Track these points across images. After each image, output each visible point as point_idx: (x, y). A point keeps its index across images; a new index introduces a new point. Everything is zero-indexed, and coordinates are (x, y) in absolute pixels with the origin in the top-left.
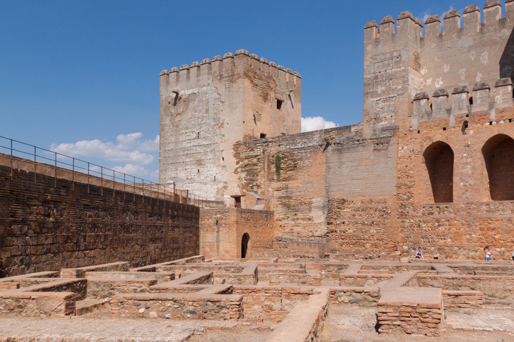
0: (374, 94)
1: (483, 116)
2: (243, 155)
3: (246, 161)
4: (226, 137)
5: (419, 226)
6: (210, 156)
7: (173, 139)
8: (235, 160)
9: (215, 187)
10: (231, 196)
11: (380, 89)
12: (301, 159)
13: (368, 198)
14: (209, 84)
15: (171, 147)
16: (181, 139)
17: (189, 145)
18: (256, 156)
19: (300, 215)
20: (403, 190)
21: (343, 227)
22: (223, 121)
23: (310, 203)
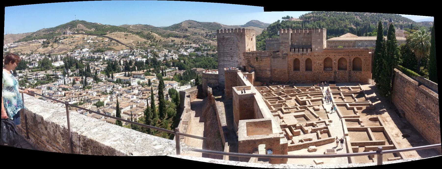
0: (282, 46)
1: (305, 54)
2: (246, 56)
3: (247, 58)
4: (240, 51)
5: (293, 76)
6: (235, 55)
7: (223, 49)
8: (243, 57)
9: (238, 63)
10: (243, 66)
11: (283, 45)
12: (263, 59)
13: (281, 69)
14: (234, 36)
15: (222, 51)
16: (225, 49)
17: (228, 51)
18: (250, 57)
19: (263, 72)
20: (289, 68)
21: (275, 75)
22: (239, 46)
23: (266, 69)
